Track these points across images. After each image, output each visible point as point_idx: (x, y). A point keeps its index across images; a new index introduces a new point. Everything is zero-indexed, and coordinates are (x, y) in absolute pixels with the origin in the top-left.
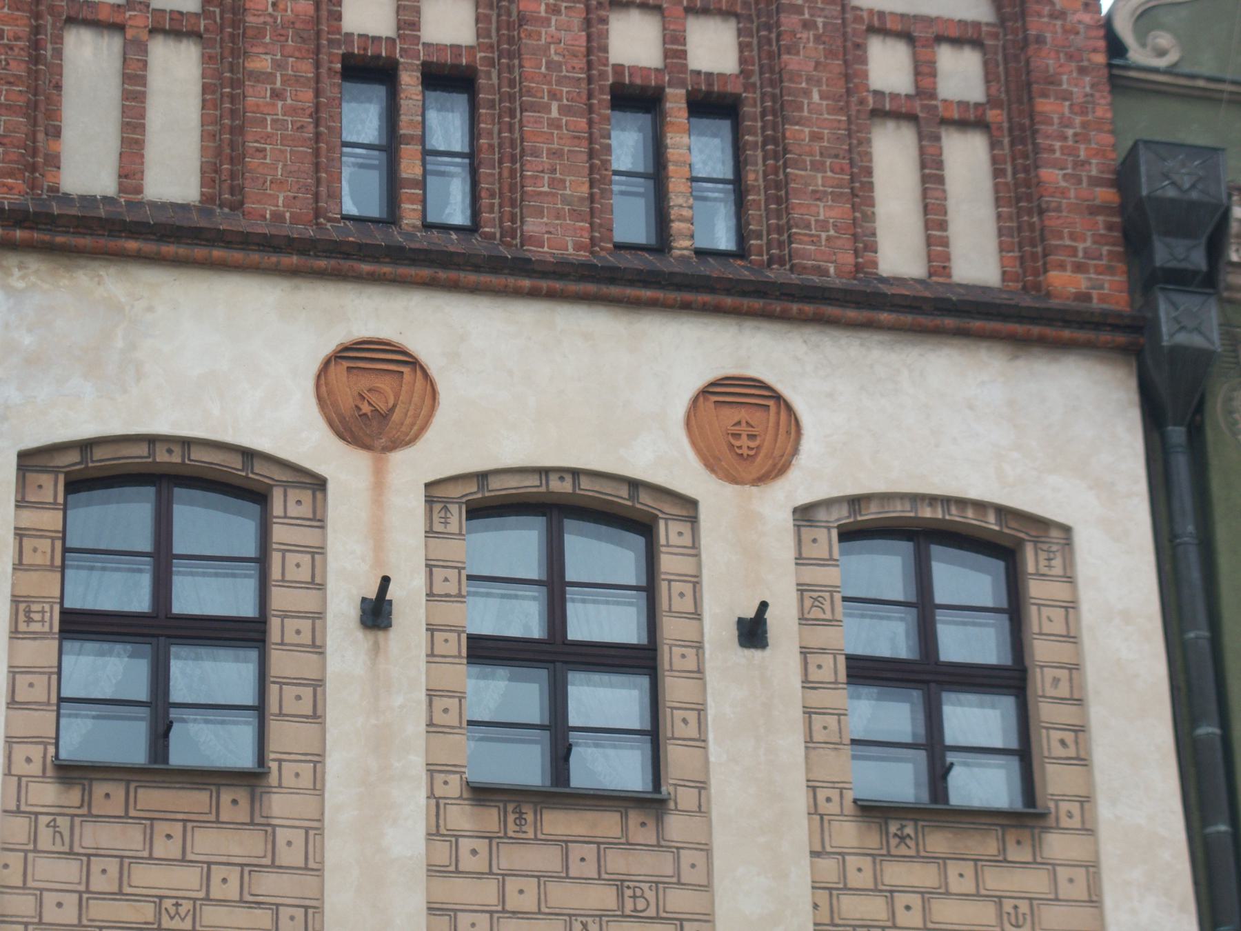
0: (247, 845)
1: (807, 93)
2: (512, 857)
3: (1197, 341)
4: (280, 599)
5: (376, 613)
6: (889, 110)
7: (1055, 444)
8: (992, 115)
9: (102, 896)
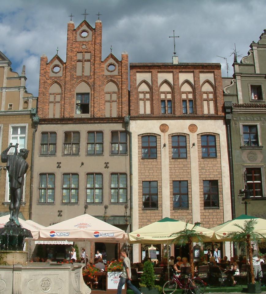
0: (156, 163)
2: (175, 163)
3: (229, 118)
4: (157, 145)
5: (165, 145)
7: (218, 127)
9: (145, 168)
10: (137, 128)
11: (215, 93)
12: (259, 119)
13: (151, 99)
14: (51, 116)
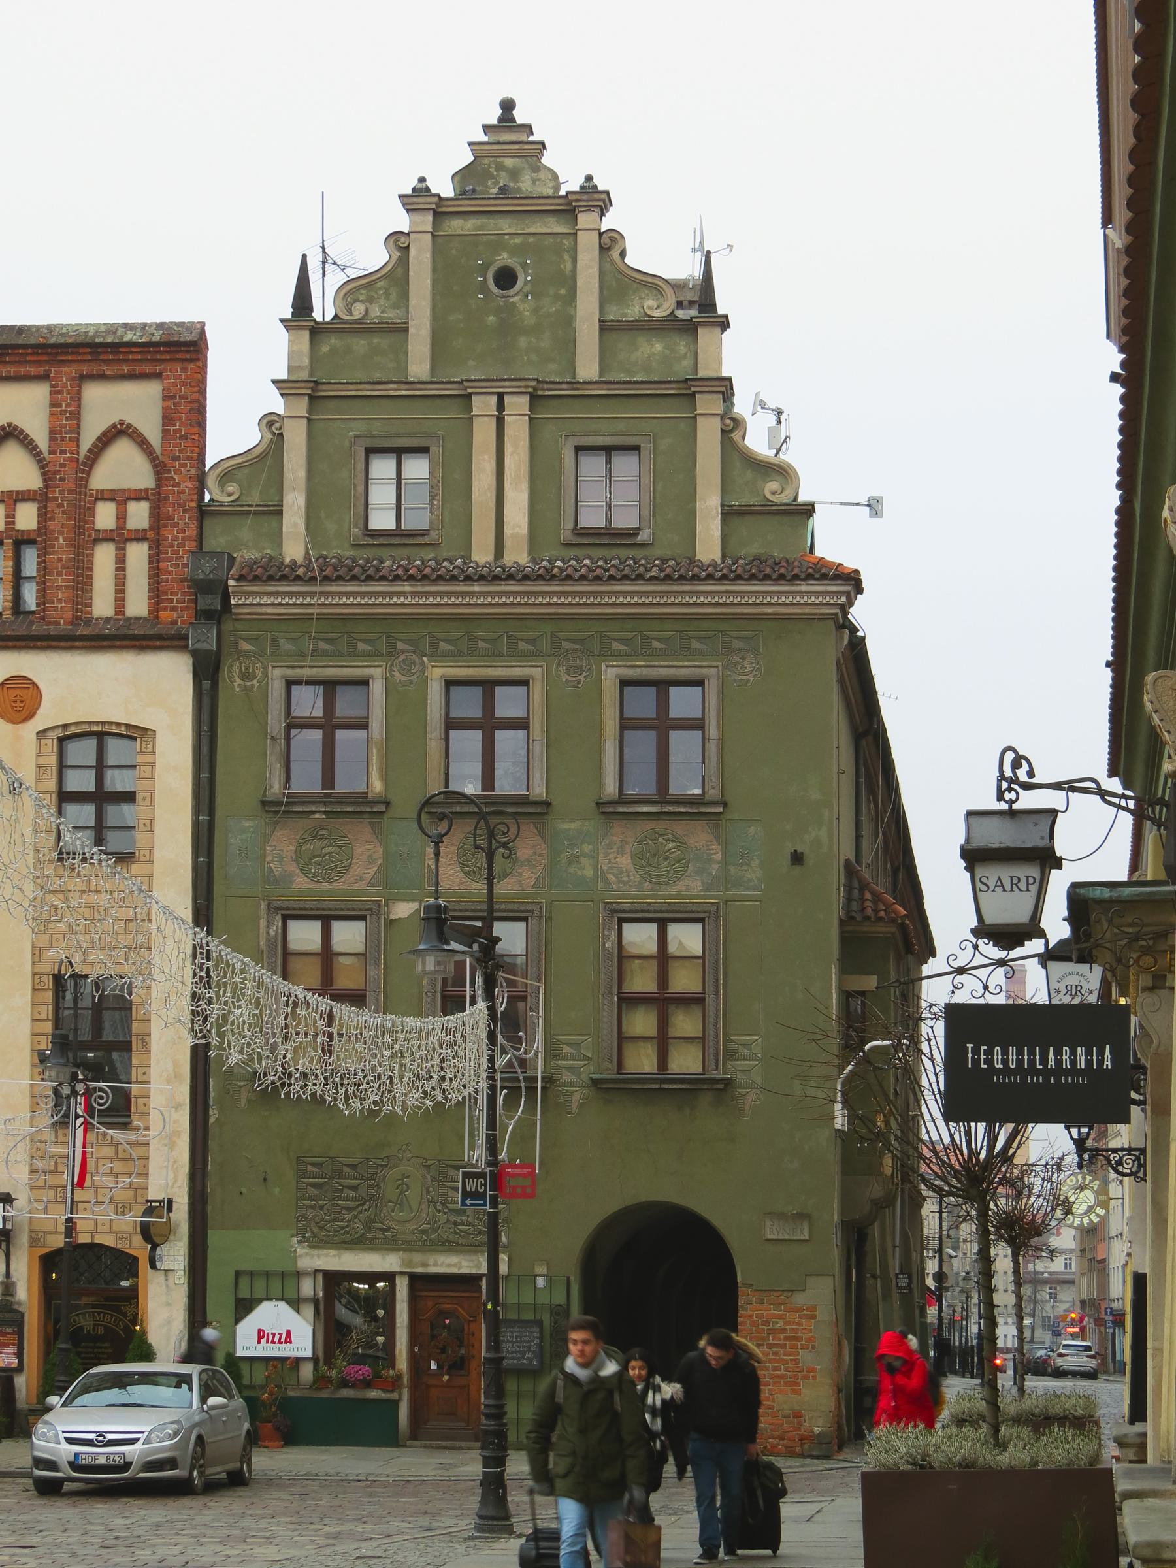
1: (57, 539)
6: (107, 537)
7: (152, 693)
8: (150, 534)
11: (156, 498)
12: (383, 645)
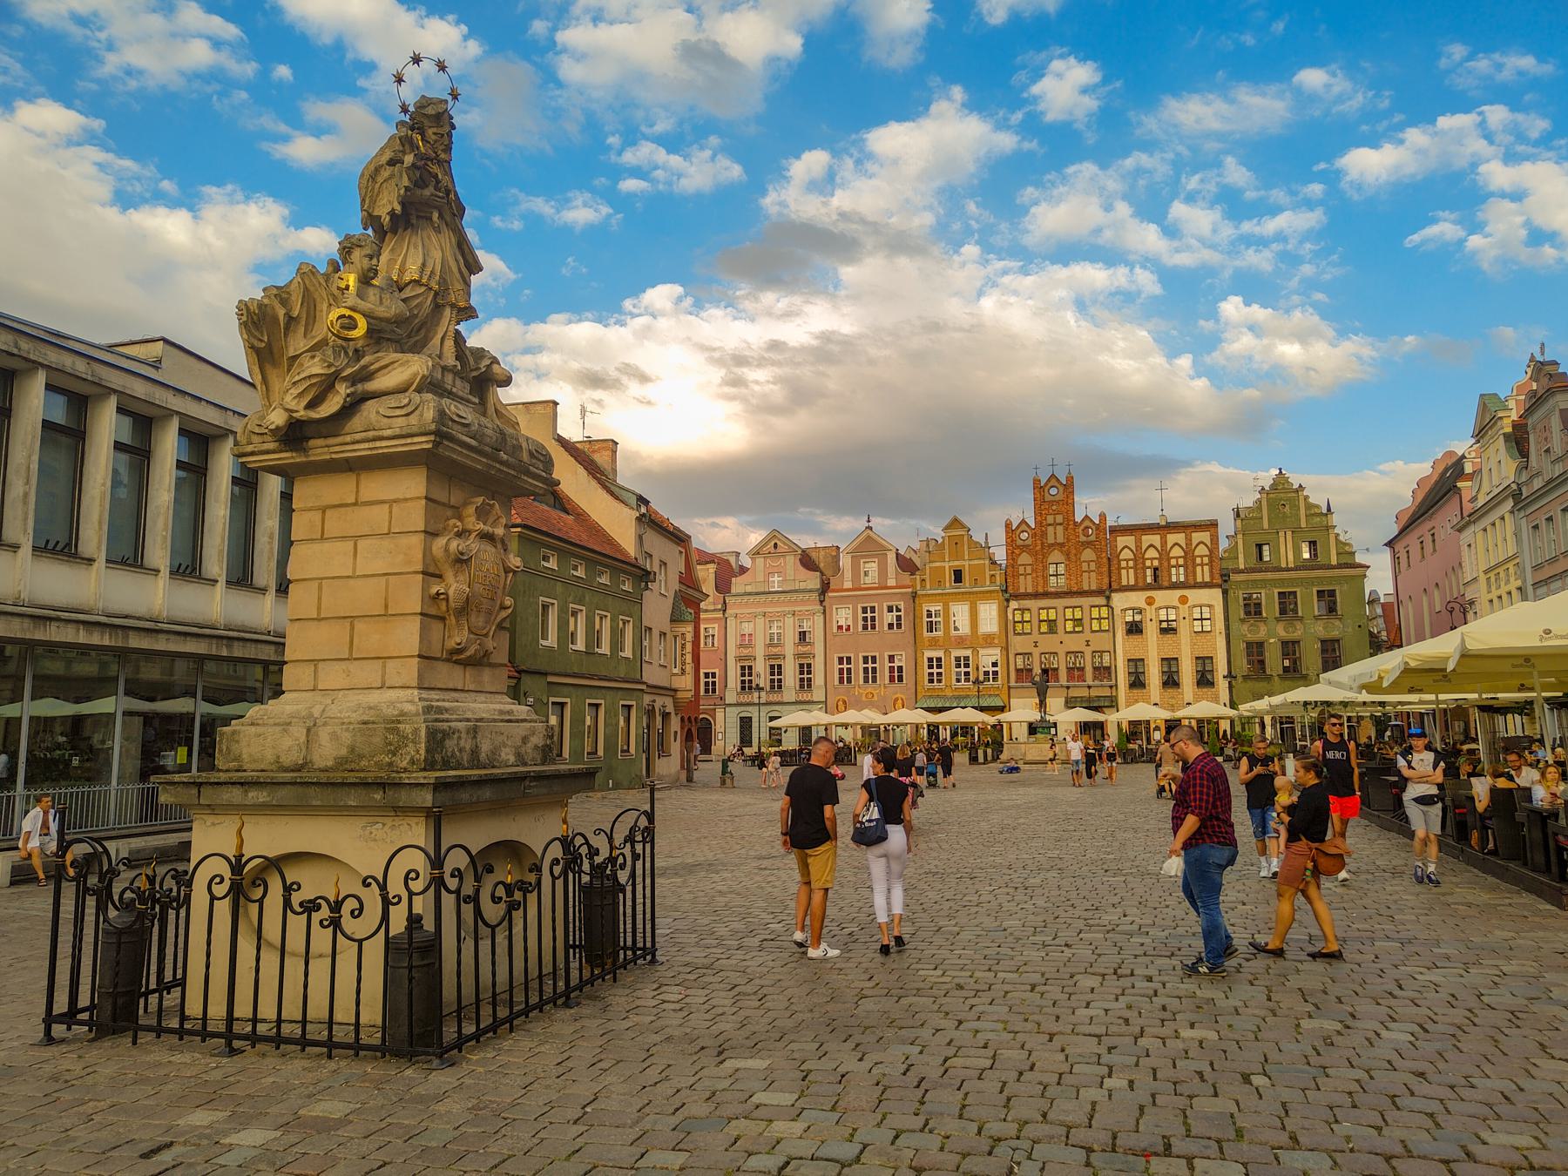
10: (1118, 600)
13: (1135, 568)
14: (1022, 590)
